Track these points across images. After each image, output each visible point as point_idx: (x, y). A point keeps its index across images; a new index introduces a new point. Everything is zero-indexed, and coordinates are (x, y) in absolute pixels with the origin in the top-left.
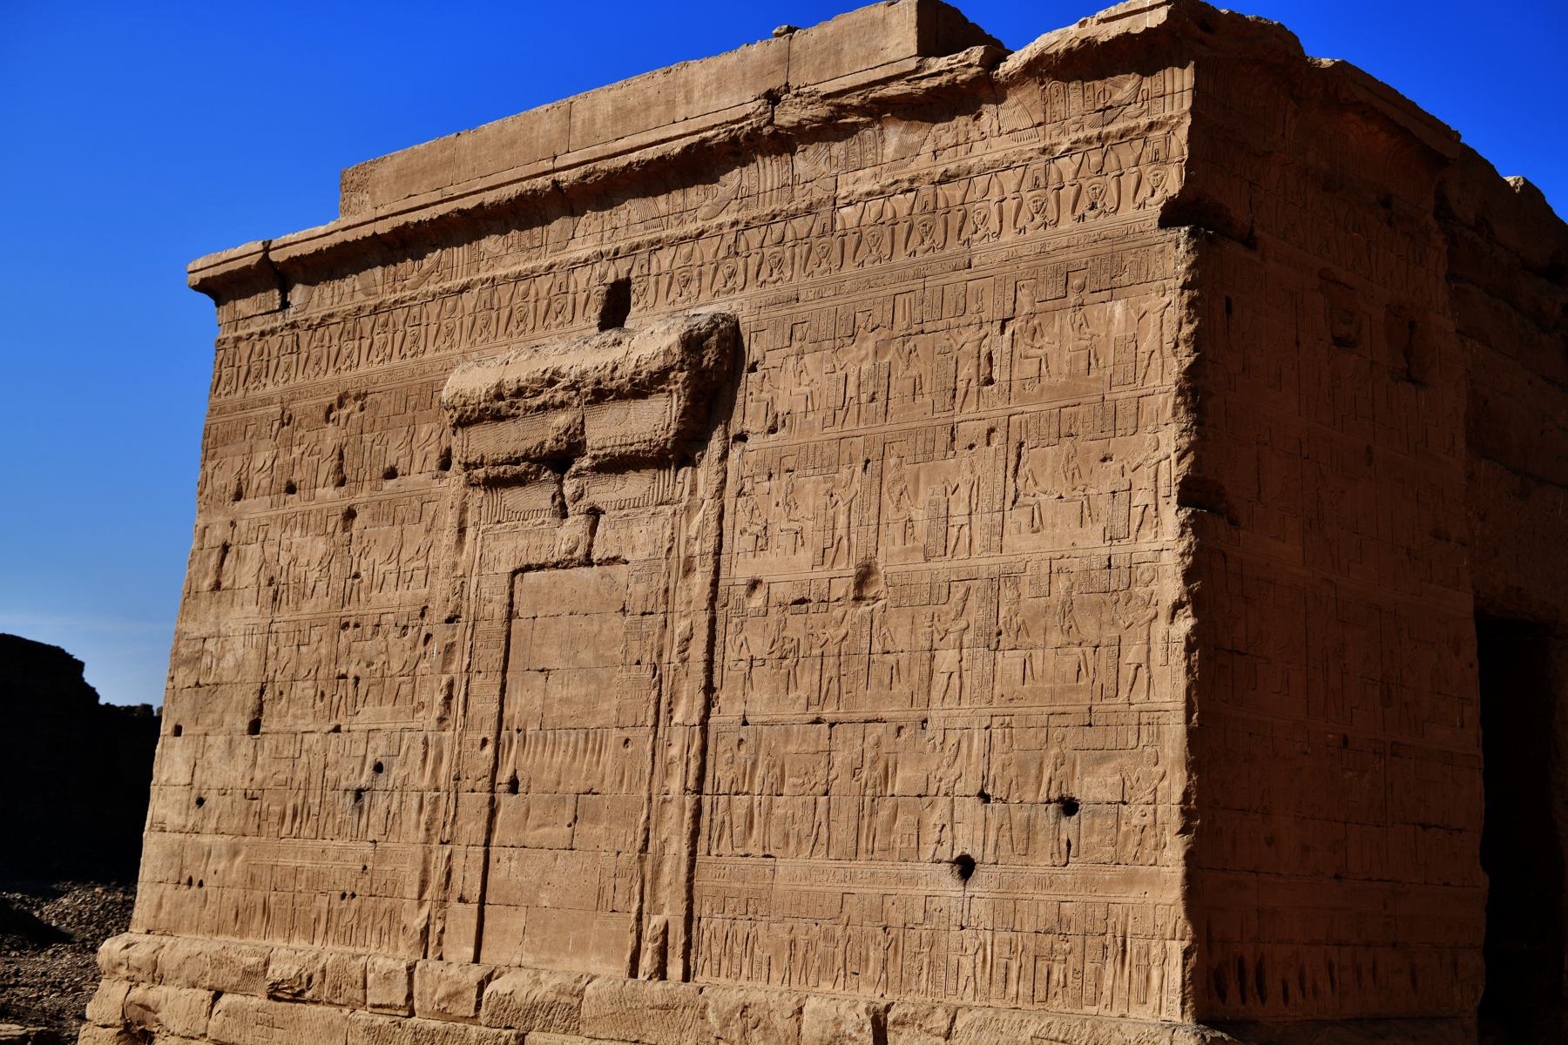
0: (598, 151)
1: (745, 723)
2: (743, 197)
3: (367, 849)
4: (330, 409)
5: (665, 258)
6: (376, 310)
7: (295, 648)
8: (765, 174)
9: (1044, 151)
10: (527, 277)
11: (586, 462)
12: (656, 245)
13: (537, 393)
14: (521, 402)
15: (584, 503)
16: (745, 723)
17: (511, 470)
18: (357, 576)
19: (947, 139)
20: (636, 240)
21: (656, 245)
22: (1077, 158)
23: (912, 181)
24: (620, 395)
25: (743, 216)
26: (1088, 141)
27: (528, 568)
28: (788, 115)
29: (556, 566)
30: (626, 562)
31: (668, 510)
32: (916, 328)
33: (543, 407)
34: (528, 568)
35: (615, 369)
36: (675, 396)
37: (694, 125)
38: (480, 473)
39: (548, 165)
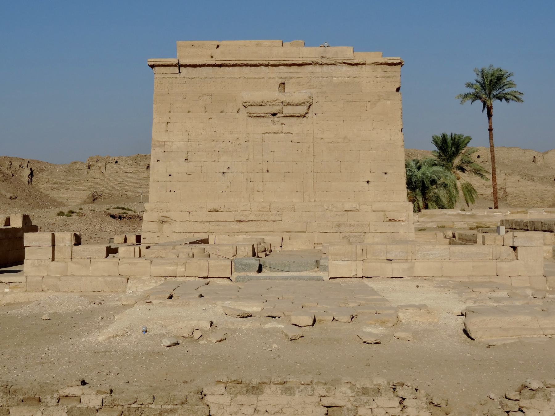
0: (280, 59)
1: (322, 161)
2: (313, 73)
3: (229, 184)
4: (200, 96)
5: (293, 80)
6: (211, 78)
7: (198, 145)
8: (317, 69)
9: (375, 76)
10: (257, 78)
11: (282, 115)
12: (291, 78)
13: (272, 102)
14: (267, 103)
15: (280, 122)
16: (322, 161)
17: (263, 115)
18: (215, 131)
19: (355, 71)
20: (287, 76)
21: (291, 78)
22: (381, 78)
23: (349, 76)
24: (293, 105)
25: (313, 76)
26: (382, 76)
27: (266, 133)
28: (324, 61)
29: (273, 133)
30: (292, 133)
31: (302, 125)
32: (351, 101)
33: (273, 105)
34: (266, 133)
35: (293, 100)
36: (306, 107)
37: (304, 59)
38: (255, 115)
39: (267, 59)
